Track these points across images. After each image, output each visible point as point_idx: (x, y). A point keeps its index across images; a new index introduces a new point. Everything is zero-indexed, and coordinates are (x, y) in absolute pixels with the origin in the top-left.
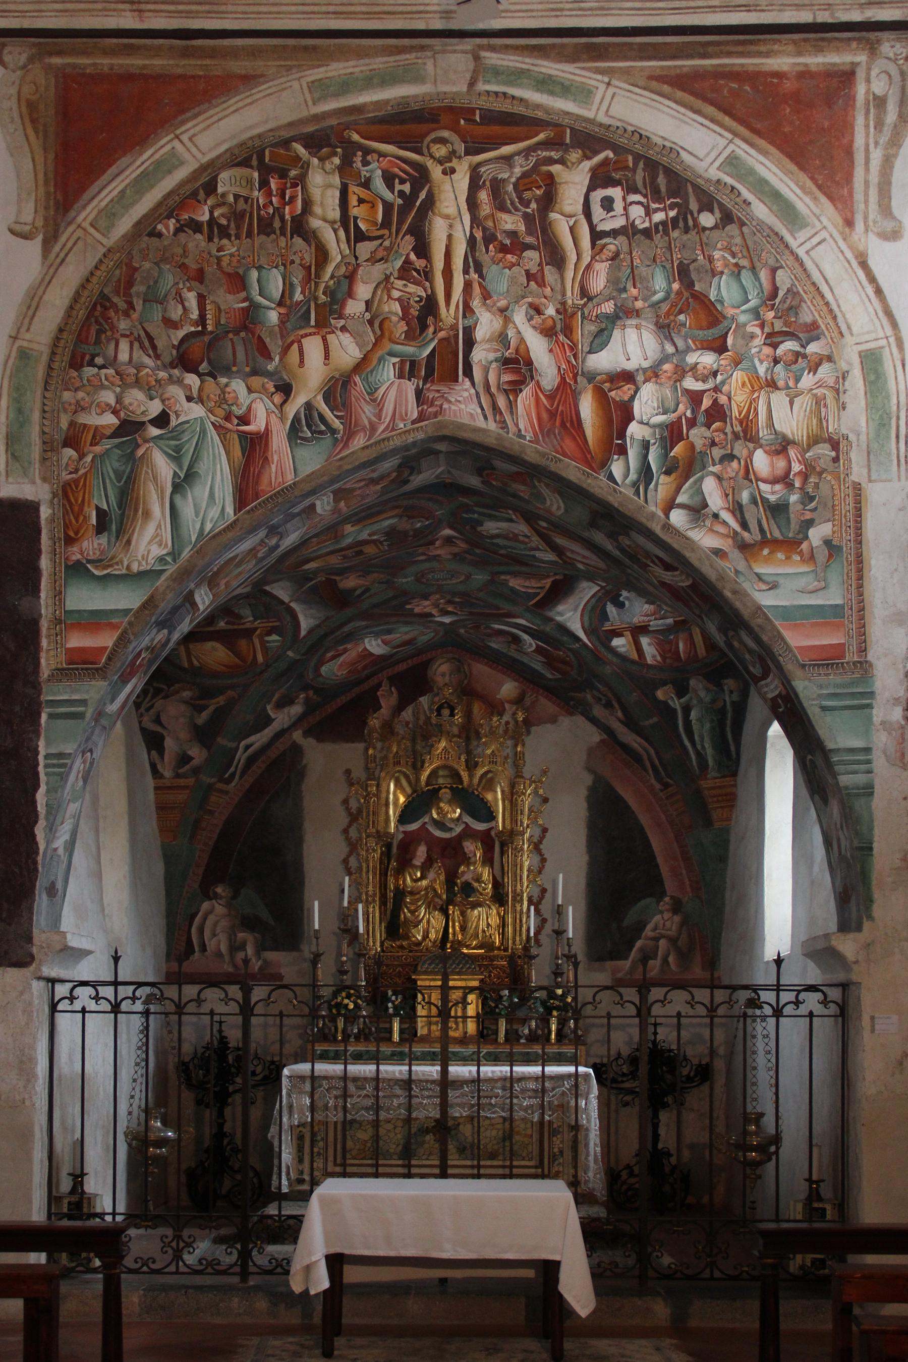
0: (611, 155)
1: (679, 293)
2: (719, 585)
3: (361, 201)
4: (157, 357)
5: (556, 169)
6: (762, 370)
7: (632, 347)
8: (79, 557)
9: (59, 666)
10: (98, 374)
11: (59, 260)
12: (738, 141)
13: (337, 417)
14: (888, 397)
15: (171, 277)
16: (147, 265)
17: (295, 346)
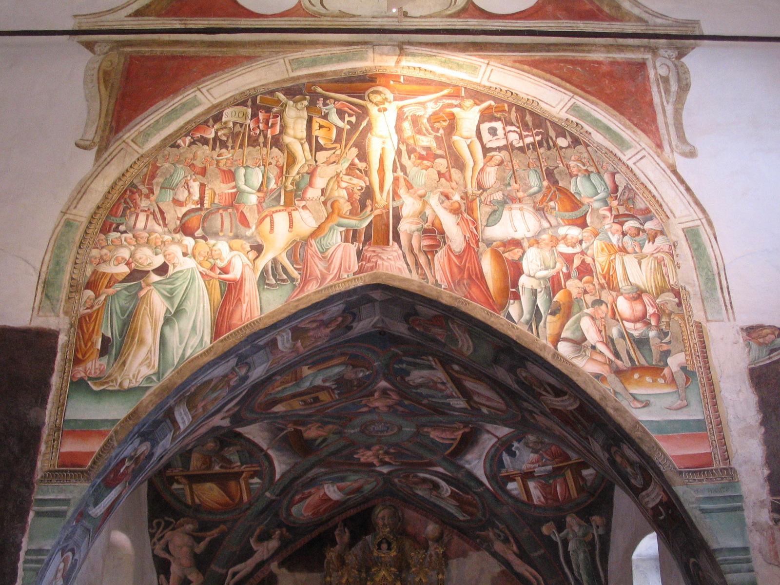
0: (493, 103)
1: (548, 188)
2: (603, 404)
3: (321, 127)
4: (165, 225)
5: (455, 110)
6: (614, 239)
7: (517, 223)
8: (83, 374)
9: (52, 468)
10: (120, 237)
11: (106, 163)
12: (576, 97)
13: (296, 269)
14: (709, 260)
15: (182, 172)
16: (167, 165)
17: (268, 219)
